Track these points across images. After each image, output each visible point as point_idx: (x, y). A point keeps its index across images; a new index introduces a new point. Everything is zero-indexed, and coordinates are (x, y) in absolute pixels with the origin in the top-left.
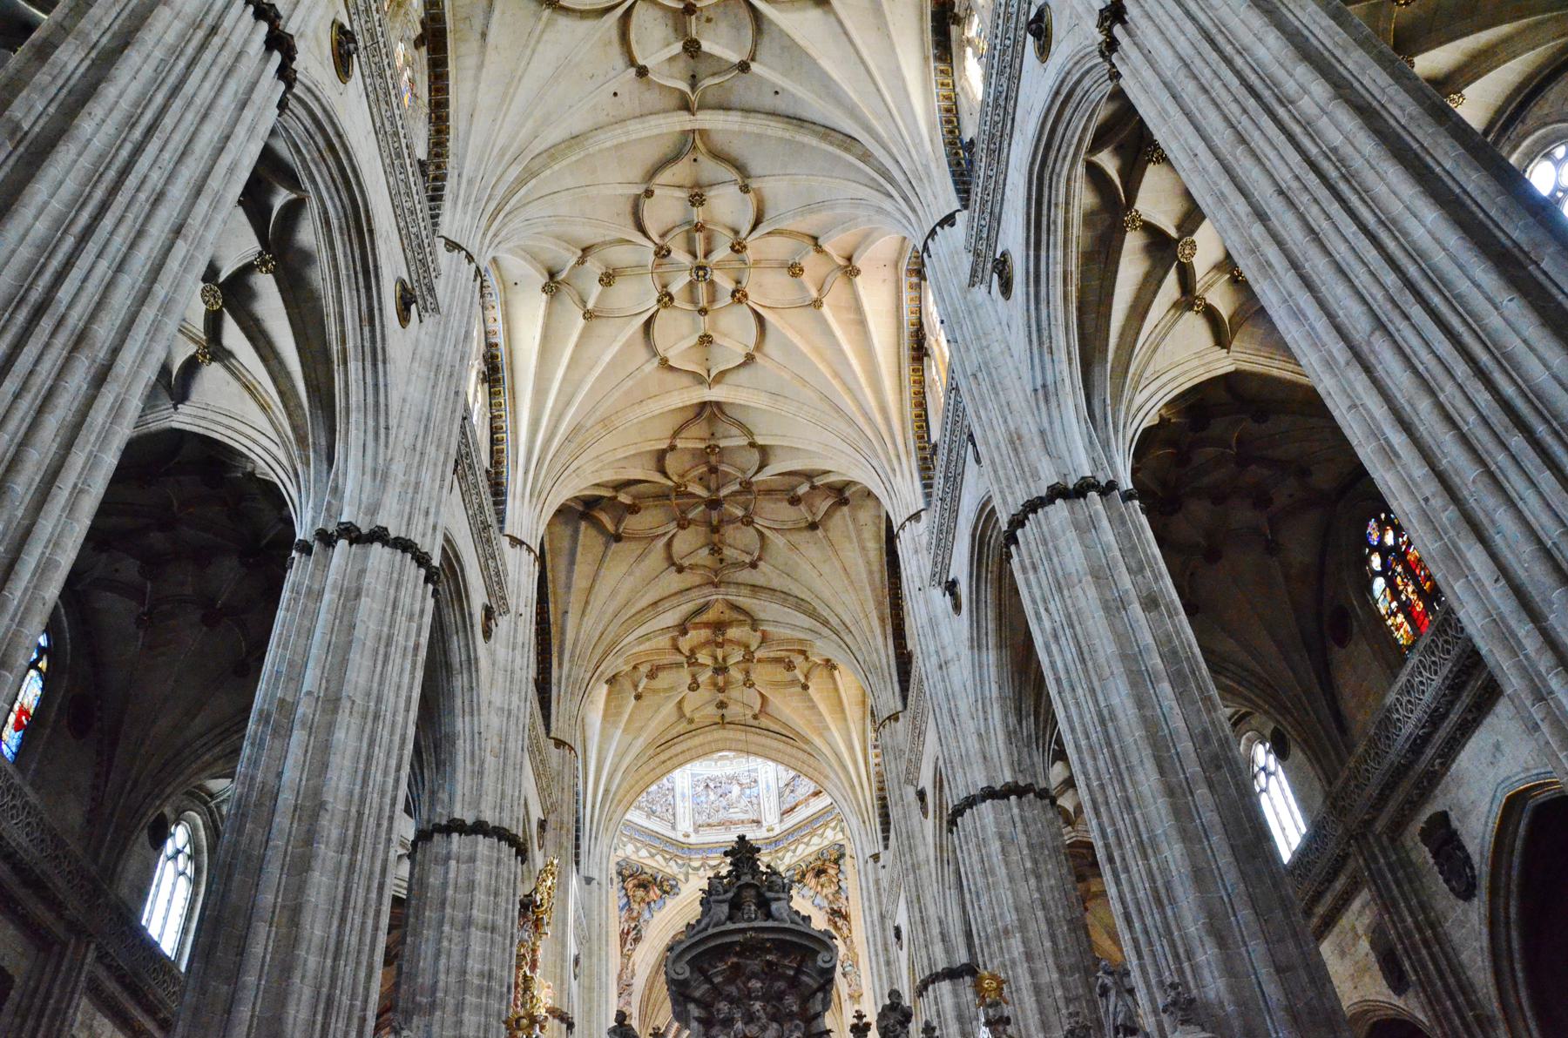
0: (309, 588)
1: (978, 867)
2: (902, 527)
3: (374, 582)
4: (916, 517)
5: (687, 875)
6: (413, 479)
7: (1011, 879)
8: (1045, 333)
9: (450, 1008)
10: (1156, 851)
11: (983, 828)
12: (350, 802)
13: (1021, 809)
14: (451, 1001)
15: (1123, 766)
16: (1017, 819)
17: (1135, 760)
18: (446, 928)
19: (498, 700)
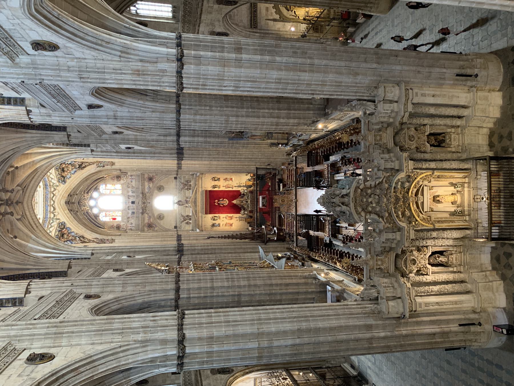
0: (207, 357)
1: (203, 124)
2: (30, 118)
3: (205, 333)
4: (29, 112)
5: (57, 219)
6: (141, 330)
7: (211, 115)
8: (100, 42)
9: (239, 290)
10: (326, 81)
11: (189, 119)
12: (293, 322)
13: (186, 105)
14: (237, 290)
15: (297, 82)
16: (190, 107)
17: (297, 78)
18: (215, 294)
19: (120, 289)
